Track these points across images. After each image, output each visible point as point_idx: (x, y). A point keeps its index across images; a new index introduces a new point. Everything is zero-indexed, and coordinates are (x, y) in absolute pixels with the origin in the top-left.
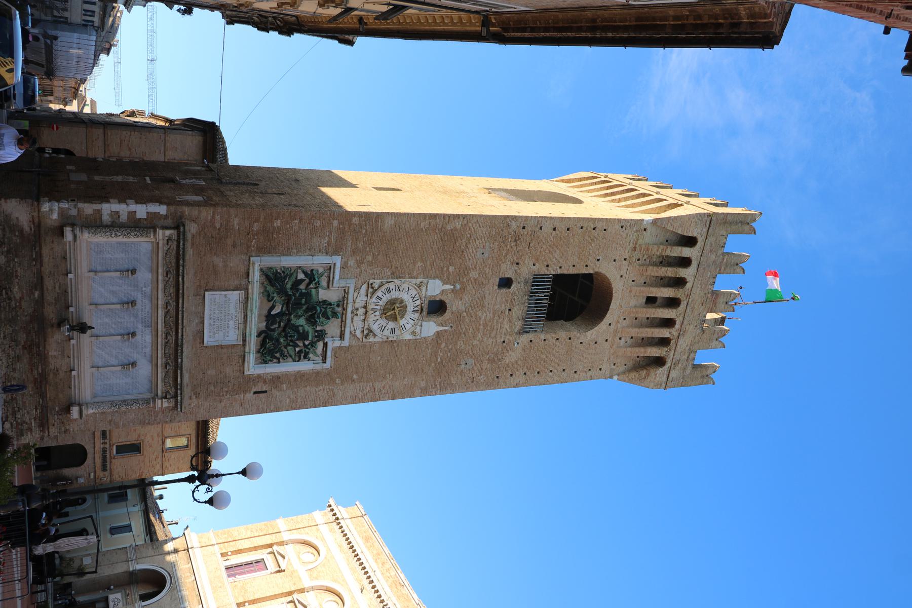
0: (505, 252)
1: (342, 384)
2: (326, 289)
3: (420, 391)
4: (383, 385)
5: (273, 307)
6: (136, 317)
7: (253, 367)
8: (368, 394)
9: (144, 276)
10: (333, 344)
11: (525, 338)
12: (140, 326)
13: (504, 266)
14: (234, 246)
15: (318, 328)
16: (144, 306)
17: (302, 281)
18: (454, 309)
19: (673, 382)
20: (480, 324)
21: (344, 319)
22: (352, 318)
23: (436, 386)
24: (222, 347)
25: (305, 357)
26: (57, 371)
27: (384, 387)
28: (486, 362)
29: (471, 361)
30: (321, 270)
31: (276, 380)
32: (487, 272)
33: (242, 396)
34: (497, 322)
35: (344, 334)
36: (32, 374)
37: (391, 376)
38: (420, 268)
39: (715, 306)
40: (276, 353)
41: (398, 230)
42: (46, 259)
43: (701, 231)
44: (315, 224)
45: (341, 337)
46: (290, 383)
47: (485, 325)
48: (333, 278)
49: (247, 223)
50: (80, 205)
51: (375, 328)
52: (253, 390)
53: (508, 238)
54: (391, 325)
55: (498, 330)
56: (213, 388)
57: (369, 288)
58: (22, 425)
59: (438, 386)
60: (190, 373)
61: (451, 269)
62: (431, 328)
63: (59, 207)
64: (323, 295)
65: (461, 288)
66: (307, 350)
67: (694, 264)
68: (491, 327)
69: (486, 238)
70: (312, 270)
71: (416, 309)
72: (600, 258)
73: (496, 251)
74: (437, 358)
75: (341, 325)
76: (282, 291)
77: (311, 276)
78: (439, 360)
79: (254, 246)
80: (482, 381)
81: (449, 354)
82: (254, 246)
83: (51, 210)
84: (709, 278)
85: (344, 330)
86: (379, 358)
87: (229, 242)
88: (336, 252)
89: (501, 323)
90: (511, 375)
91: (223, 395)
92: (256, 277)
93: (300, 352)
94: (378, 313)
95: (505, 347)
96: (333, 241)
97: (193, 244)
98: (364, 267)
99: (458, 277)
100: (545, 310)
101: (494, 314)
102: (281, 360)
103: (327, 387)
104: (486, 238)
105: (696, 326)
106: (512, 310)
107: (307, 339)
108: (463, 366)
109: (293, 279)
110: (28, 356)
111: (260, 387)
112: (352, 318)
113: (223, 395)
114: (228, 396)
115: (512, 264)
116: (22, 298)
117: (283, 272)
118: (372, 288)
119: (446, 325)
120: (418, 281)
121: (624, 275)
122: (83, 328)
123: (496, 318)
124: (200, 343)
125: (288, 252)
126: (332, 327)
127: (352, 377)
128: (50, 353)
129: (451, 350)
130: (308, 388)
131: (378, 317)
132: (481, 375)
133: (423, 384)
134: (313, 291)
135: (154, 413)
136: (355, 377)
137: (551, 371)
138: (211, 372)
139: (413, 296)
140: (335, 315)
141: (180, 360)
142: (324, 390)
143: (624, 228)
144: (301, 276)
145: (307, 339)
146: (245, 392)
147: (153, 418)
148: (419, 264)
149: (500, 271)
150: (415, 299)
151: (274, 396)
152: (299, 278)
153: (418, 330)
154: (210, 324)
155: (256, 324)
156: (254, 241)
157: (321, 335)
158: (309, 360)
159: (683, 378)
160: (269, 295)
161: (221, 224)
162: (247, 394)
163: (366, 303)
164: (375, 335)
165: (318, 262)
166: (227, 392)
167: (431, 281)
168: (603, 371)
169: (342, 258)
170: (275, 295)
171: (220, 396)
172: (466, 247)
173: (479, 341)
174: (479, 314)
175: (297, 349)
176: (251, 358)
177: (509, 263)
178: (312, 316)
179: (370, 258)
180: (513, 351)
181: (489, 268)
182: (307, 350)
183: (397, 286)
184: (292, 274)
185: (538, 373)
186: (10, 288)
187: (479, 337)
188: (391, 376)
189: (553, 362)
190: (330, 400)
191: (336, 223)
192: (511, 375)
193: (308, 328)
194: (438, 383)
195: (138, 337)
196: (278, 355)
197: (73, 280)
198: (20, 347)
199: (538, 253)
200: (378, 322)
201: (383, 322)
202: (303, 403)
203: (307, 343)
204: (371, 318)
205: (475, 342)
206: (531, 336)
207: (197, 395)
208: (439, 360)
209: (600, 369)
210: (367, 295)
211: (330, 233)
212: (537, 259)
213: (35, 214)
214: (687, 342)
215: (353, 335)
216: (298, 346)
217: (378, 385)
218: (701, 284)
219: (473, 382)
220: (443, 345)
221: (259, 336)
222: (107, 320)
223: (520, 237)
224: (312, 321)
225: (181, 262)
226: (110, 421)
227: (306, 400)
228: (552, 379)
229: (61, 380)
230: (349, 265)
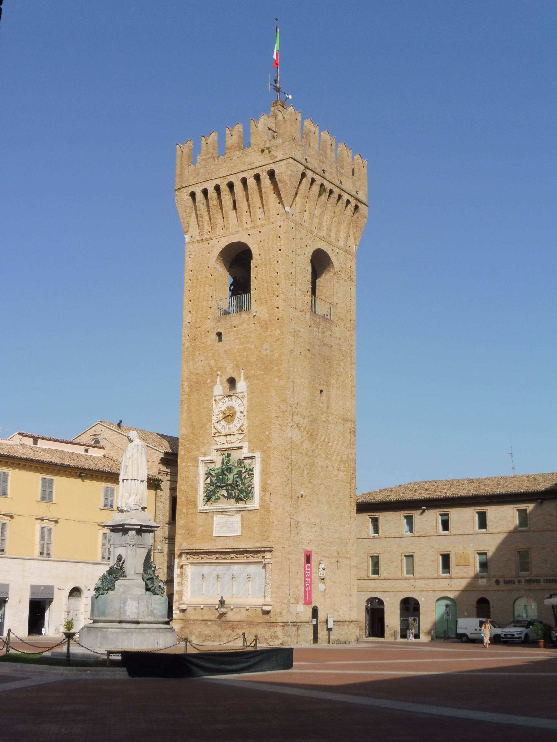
0: (201, 345)
1: (271, 441)
2: (216, 464)
3: (281, 381)
4: (274, 411)
5: (223, 496)
6: (225, 574)
7: (256, 503)
8: (279, 421)
9: (206, 569)
10: (246, 452)
11: (254, 306)
12: (230, 572)
13: (209, 342)
14: (193, 522)
15: (236, 465)
16: (220, 569)
17: (211, 480)
18: (232, 371)
19: (287, 152)
20: (242, 348)
21: (232, 449)
22: (232, 443)
23: (279, 370)
24: (242, 524)
25: (252, 471)
26: (248, 616)
27: (275, 410)
28: (266, 333)
29: (265, 346)
30: (206, 469)
31: (264, 488)
32: (211, 354)
33: (271, 509)
34: (241, 335)
35: (240, 447)
36: (246, 629)
37: (269, 406)
38: (208, 403)
39: (232, 146)
40: (248, 490)
41: (188, 424)
42: (196, 618)
43: (185, 193)
44: (184, 476)
45: (242, 449)
46: (266, 479)
47: (242, 343)
48: (209, 460)
49: (183, 516)
50: (174, 601)
51: (238, 426)
52: (269, 502)
53: (194, 345)
54: (238, 415)
55: (247, 331)
56: (265, 529)
57: (216, 435)
58: (272, 636)
59: (279, 367)
60: (255, 542)
61: (209, 381)
62: (242, 385)
63: (175, 610)
64: (218, 465)
65: (220, 370)
66: (248, 470)
67: (205, 186)
68: (244, 338)
69: (193, 362)
70: (206, 474)
71: (230, 400)
72: (207, 267)
73: (200, 352)
74: (261, 374)
75: (236, 449)
76: (214, 492)
77: (209, 474)
78: (262, 372)
79: (193, 511)
80: (279, 332)
81: (259, 365)
82: (193, 511)
83: (176, 614)
84: (214, 165)
85: (238, 447)
86: (257, 418)
87: (191, 524)
88: (197, 461)
89: (242, 331)
90: (278, 308)
91: (270, 521)
92: (207, 508)
93: (249, 475)
94: (231, 426)
95: (257, 321)
96: (192, 464)
97: (191, 544)
98: (206, 442)
99: (214, 374)
100: (238, 297)
101: (236, 339)
102: (252, 486)
103: (272, 452)
104: (193, 362)
105: (246, 155)
106: (235, 326)
107: (241, 471)
108: (268, 352)
109: (209, 485)
110: (237, 630)
111: (267, 498)
112: (232, 443)
113: (270, 521)
114: (270, 518)
115: (207, 336)
116: (211, 630)
117: (206, 491)
118: (216, 433)
119: (241, 374)
120: (214, 402)
121: (218, 240)
122: (222, 603)
123: (239, 336)
124: (240, 537)
125: (196, 490)
126: (236, 456)
127: (267, 435)
128: (239, 619)
129: (256, 365)
130: (271, 465)
131: (233, 425)
132: (275, 335)
133: (276, 380)
134: (216, 471)
135: (275, 563)
136: (267, 433)
137: (277, 273)
138: (256, 530)
139: (222, 403)
140: (229, 456)
141: (242, 550)
142: (273, 454)
143: (190, 256)
144: (208, 481)
145: (241, 471)
146: (269, 507)
147: (278, 563)
148: (205, 404)
149: (212, 344)
150: (224, 402)
151: (273, 488)
152: (209, 482)
153: (241, 395)
154: (230, 532)
155: (232, 504)
156: (191, 511)
157: (240, 462)
158: (254, 467)
159: (284, 143)
160: (217, 499)
161: (183, 530)
162: (271, 506)
163: (224, 435)
164: (243, 425)
165: (202, 471)
166: (268, 519)
167: (215, 394)
168: (281, 223)
169: (201, 457)
170: (216, 495)
171: (270, 524)
172: (198, 374)
173: (252, 345)
174: (235, 351)
175: (247, 476)
176: (249, 505)
177: (207, 339)
178: (227, 470)
179: (201, 438)
180: (261, 313)
181: (209, 353)
182: (248, 470)
183: (217, 417)
184: (207, 487)
185: (278, 284)
186: (206, 635)
187: (249, 345)
188: (269, 406)
189: (270, 275)
190: (280, 448)
191: (184, 464)
192: (278, 308)
193: (235, 471)
194: (277, 368)
195: (235, 572)
196: (249, 489)
197: (204, 605)
198: (232, 633)
199: (202, 319)
200: (236, 425)
201: (236, 420)
202: (280, 467)
203: (244, 471)
204: (234, 430)
205: (253, 347)
206: (252, 302)
207: (268, 537)
208: (262, 372)
209: (280, 227)
210: (220, 436)
211: (188, 466)
212: (206, 318)
213: (177, 621)
214: (258, 157)
215: (241, 441)
216: (245, 476)
217: (274, 414)
218: (218, 170)
219: (279, 339)
220: (253, 372)
221: (238, 502)
222: (226, 589)
223: (193, 337)
224: (230, 470)
225: (194, 551)
226: (278, 589)
227: (278, 466)
228: (283, 270)
229: (252, 614)
230: (204, 451)
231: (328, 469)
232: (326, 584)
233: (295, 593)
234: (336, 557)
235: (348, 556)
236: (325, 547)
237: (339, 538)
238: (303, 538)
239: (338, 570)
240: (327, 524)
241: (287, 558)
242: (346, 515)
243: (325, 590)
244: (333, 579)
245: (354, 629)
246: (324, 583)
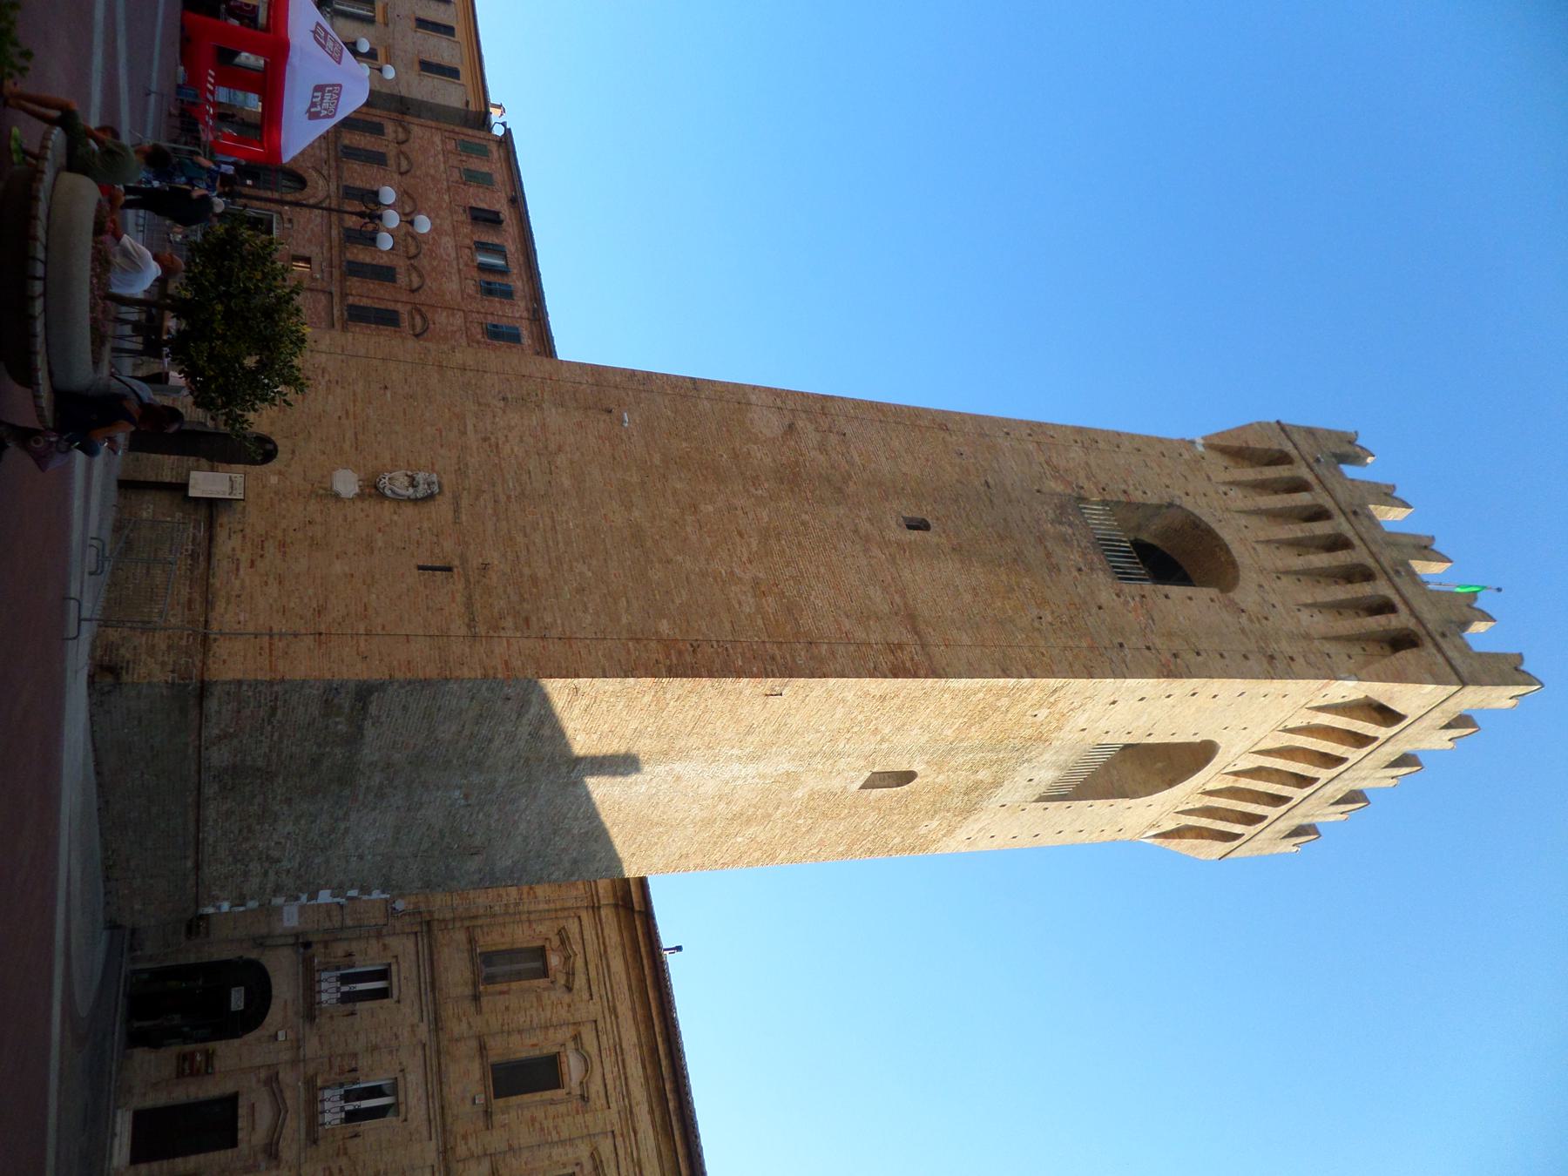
231: (738, 539)
232: (359, 504)
233: (320, 372)
234: (464, 559)
235: (481, 629)
236: (490, 511)
237: (534, 580)
238: (497, 419)
239: (420, 568)
240: (567, 522)
241: (425, 354)
242: (624, 621)
243: (337, 497)
244: (380, 540)
245: (170, 647)
246: (361, 496)
